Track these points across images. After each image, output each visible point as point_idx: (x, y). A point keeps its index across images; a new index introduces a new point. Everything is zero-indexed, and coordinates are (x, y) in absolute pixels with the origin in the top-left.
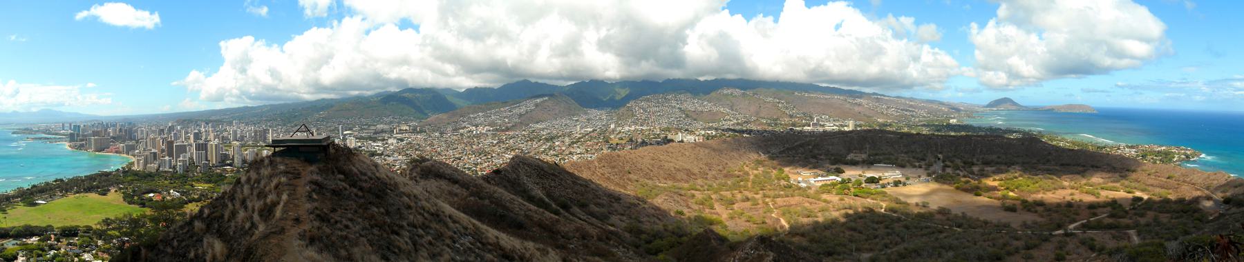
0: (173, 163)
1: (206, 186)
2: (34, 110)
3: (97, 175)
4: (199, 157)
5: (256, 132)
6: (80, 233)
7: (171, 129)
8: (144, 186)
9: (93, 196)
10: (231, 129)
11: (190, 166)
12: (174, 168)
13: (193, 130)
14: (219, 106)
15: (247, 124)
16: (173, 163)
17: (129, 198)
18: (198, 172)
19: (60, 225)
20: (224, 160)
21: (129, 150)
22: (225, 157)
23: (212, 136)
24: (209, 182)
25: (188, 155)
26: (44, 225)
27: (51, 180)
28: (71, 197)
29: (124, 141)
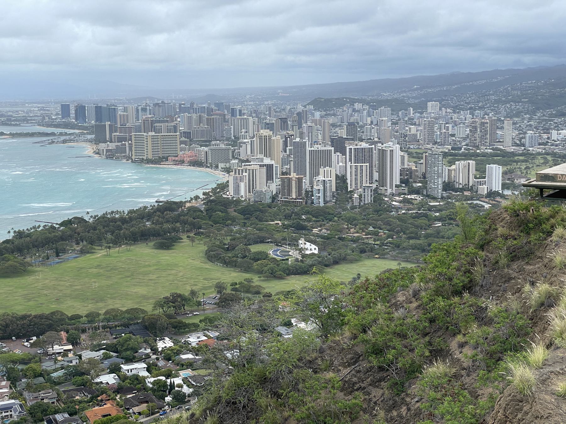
12: (309, 194)
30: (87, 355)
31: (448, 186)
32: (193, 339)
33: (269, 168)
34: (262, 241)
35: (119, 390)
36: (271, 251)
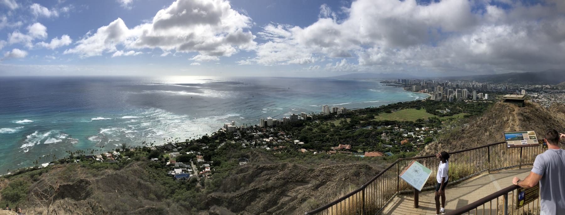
30: (401, 130)
32: (423, 129)
34: (438, 109)
35: (407, 137)
36: (440, 111)
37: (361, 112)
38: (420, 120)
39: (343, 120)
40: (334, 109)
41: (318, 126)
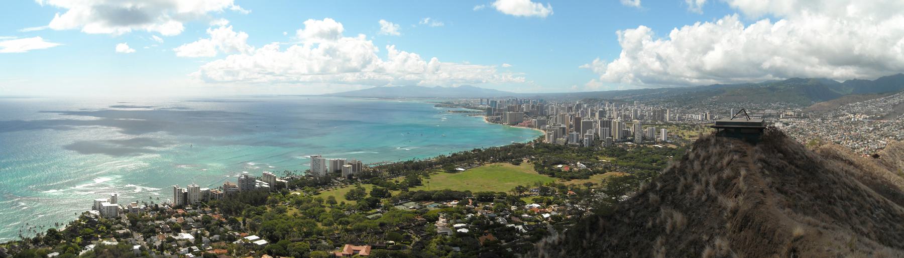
0: (580, 137)
1: (610, 159)
2: (455, 86)
3: (512, 146)
4: (603, 133)
5: (654, 112)
6: (495, 199)
7: (579, 107)
8: (554, 158)
9: (507, 165)
10: (632, 109)
11: (595, 141)
12: (581, 142)
13: (598, 108)
14: (621, 88)
15: (647, 105)
16: (580, 137)
17: (540, 168)
18: (602, 148)
19: (477, 191)
20: (625, 136)
21: (541, 124)
22: (628, 133)
23: (614, 114)
24: (612, 155)
25: (594, 131)
26: (463, 190)
27: (469, 150)
28: (488, 165)
29: (535, 117)
31: (644, 138)
33: (564, 128)
37: (395, 170)
38: (520, 189)
39: (353, 187)
40: (335, 162)
41: (298, 203)
